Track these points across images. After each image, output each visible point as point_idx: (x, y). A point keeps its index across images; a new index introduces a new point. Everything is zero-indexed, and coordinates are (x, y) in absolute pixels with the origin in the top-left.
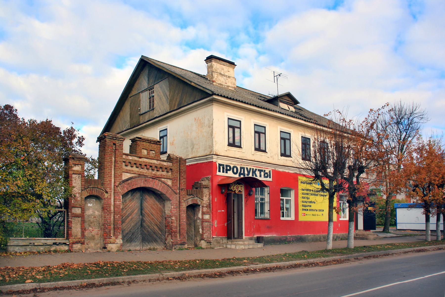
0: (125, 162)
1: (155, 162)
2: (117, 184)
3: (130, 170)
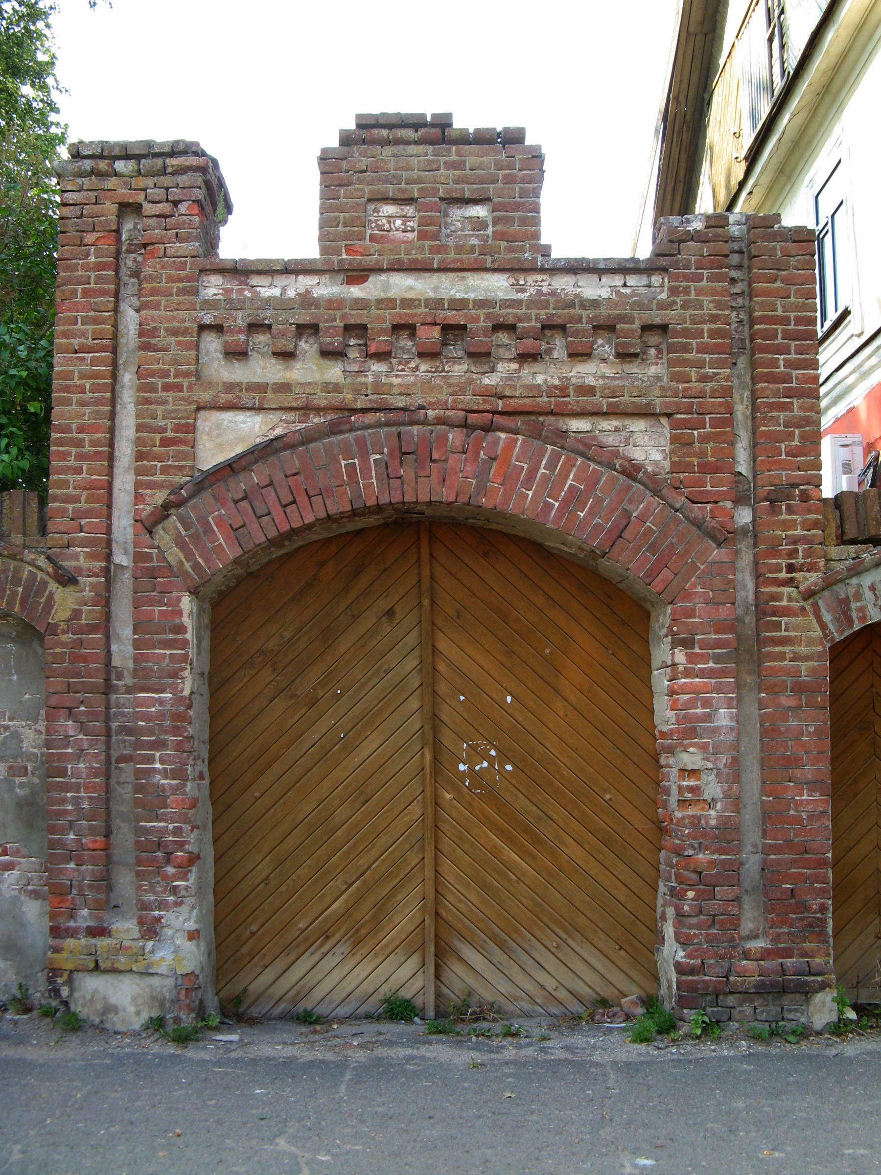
0: (218, 328)
1: (496, 286)
2: (147, 510)
3: (260, 388)
